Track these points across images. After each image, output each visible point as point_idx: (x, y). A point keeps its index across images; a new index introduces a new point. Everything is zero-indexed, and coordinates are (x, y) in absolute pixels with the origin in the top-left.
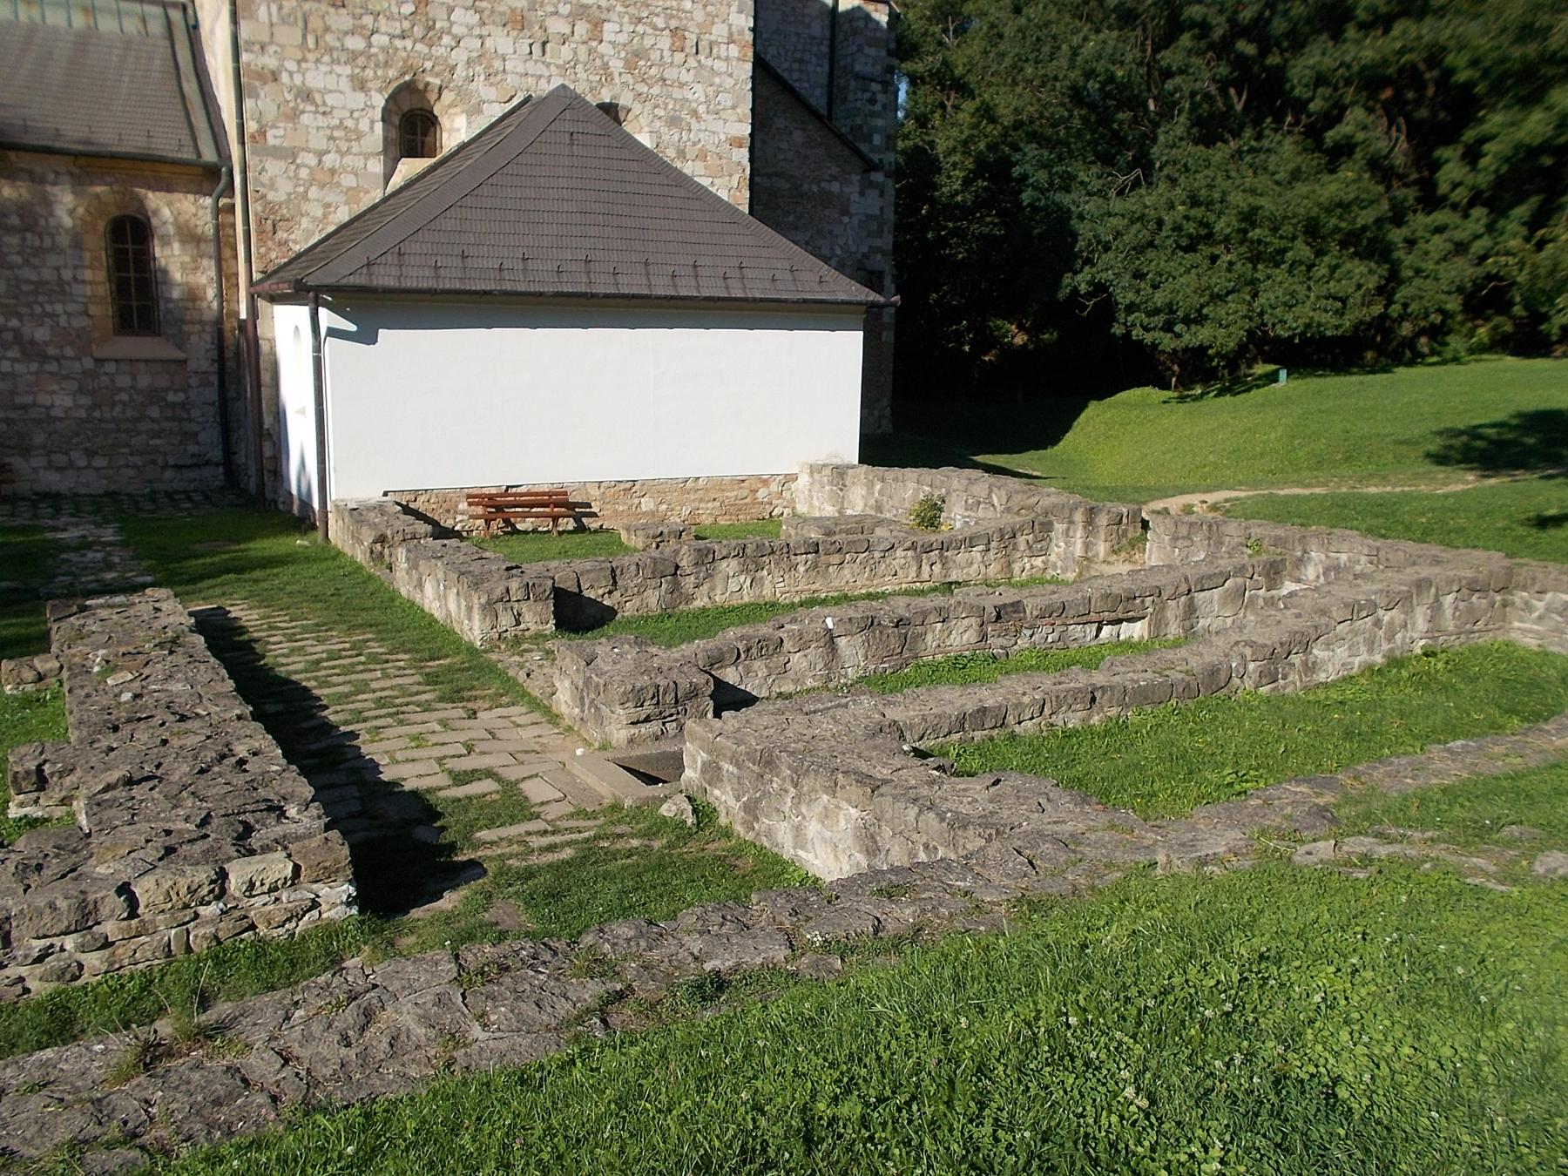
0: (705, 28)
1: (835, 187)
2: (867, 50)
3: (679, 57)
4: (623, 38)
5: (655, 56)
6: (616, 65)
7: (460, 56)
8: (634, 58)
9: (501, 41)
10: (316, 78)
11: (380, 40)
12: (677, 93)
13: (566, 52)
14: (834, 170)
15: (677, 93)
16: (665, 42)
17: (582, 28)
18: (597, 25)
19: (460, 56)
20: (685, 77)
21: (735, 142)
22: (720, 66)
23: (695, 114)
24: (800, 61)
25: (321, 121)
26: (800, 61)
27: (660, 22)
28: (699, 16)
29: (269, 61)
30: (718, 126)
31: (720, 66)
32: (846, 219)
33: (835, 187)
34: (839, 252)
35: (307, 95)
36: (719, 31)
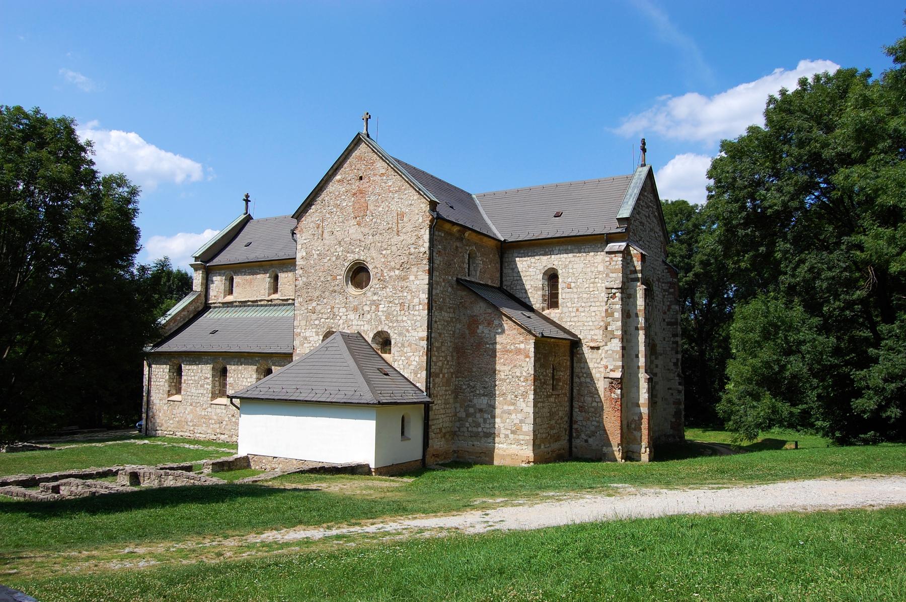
0: (411, 301)
1: (522, 346)
2: (611, 275)
3: (403, 312)
4: (385, 309)
5: (395, 313)
6: (383, 318)
7: (341, 322)
8: (388, 315)
9: (352, 316)
10: (308, 334)
11: (323, 320)
12: (402, 324)
13: (369, 316)
14: (522, 339)
15: (402, 324)
16: (398, 308)
17: (373, 307)
18: (377, 306)
19: (341, 322)
20: (405, 318)
21: (422, 339)
22: (416, 313)
23: (408, 331)
24: (593, 283)
25: (308, 345)
26: (593, 283)
27: (397, 302)
28: (409, 297)
29: (299, 330)
30: (415, 334)
31: (416, 313)
32: (528, 360)
33: (522, 346)
34: (524, 374)
35: (306, 338)
36: (416, 301)
